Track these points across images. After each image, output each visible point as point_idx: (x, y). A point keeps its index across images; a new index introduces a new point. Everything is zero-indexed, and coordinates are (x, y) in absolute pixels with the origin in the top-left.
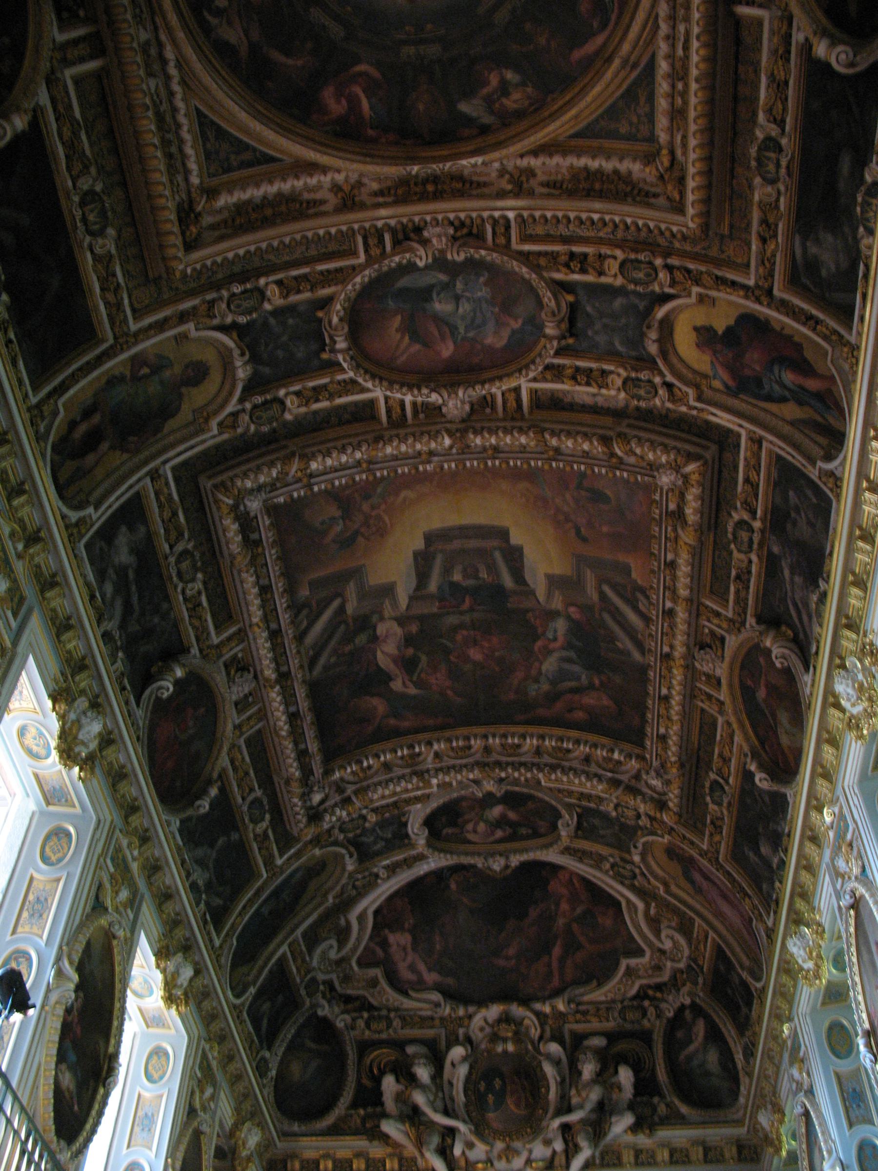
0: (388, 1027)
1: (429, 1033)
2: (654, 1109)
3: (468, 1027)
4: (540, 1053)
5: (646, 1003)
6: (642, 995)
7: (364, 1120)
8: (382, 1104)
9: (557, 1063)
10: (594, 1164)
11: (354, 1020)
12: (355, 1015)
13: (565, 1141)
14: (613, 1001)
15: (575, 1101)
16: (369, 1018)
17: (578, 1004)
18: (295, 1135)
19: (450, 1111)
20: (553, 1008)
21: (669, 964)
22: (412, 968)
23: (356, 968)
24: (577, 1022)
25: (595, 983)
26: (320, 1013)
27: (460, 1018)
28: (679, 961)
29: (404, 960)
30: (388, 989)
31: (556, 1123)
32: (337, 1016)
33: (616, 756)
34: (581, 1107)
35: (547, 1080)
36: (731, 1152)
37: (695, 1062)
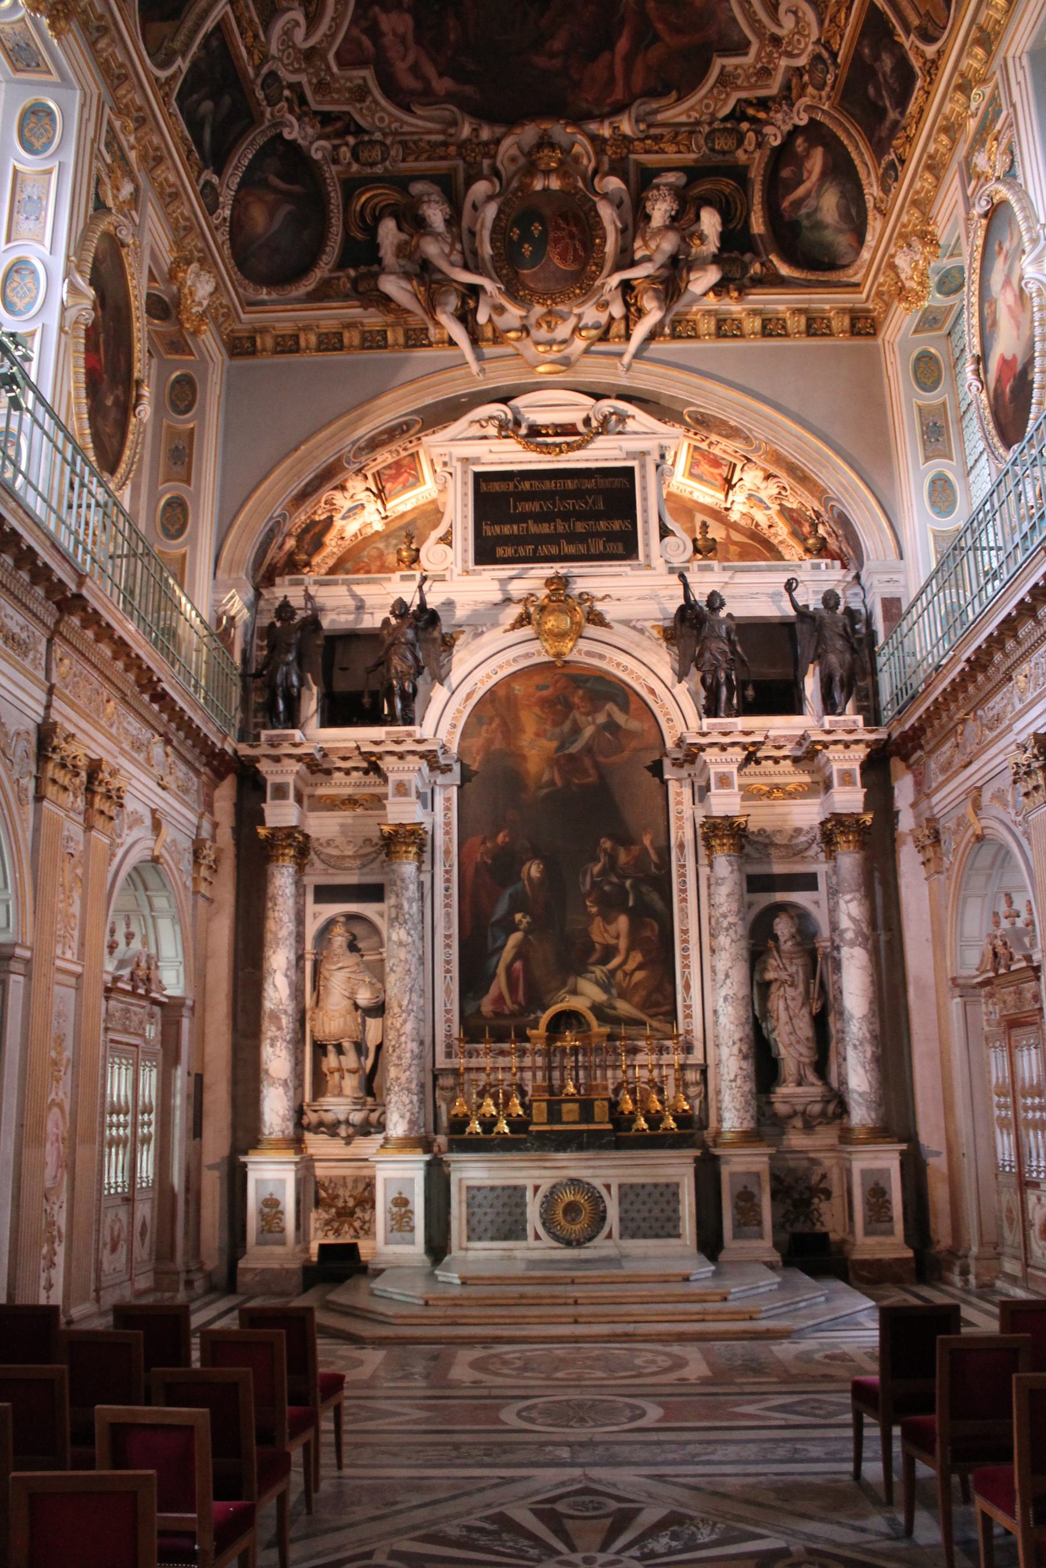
0: (384, 160)
2: (745, 268)
3: (494, 157)
4: (597, 194)
5: (745, 126)
6: (737, 115)
7: (355, 282)
8: (379, 261)
10: (662, 334)
11: (336, 148)
12: (336, 142)
13: (627, 305)
14: (698, 123)
15: (638, 255)
16: (356, 145)
17: (650, 126)
18: (263, 303)
19: (471, 265)
21: (784, 62)
22: (415, 70)
23: (335, 69)
24: (647, 152)
25: (674, 95)
26: (287, 136)
27: (486, 144)
28: (798, 55)
29: (403, 59)
30: (383, 102)
31: (615, 280)
32: (311, 143)
34: (648, 259)
35: (603, 228)
37: (803, 211)
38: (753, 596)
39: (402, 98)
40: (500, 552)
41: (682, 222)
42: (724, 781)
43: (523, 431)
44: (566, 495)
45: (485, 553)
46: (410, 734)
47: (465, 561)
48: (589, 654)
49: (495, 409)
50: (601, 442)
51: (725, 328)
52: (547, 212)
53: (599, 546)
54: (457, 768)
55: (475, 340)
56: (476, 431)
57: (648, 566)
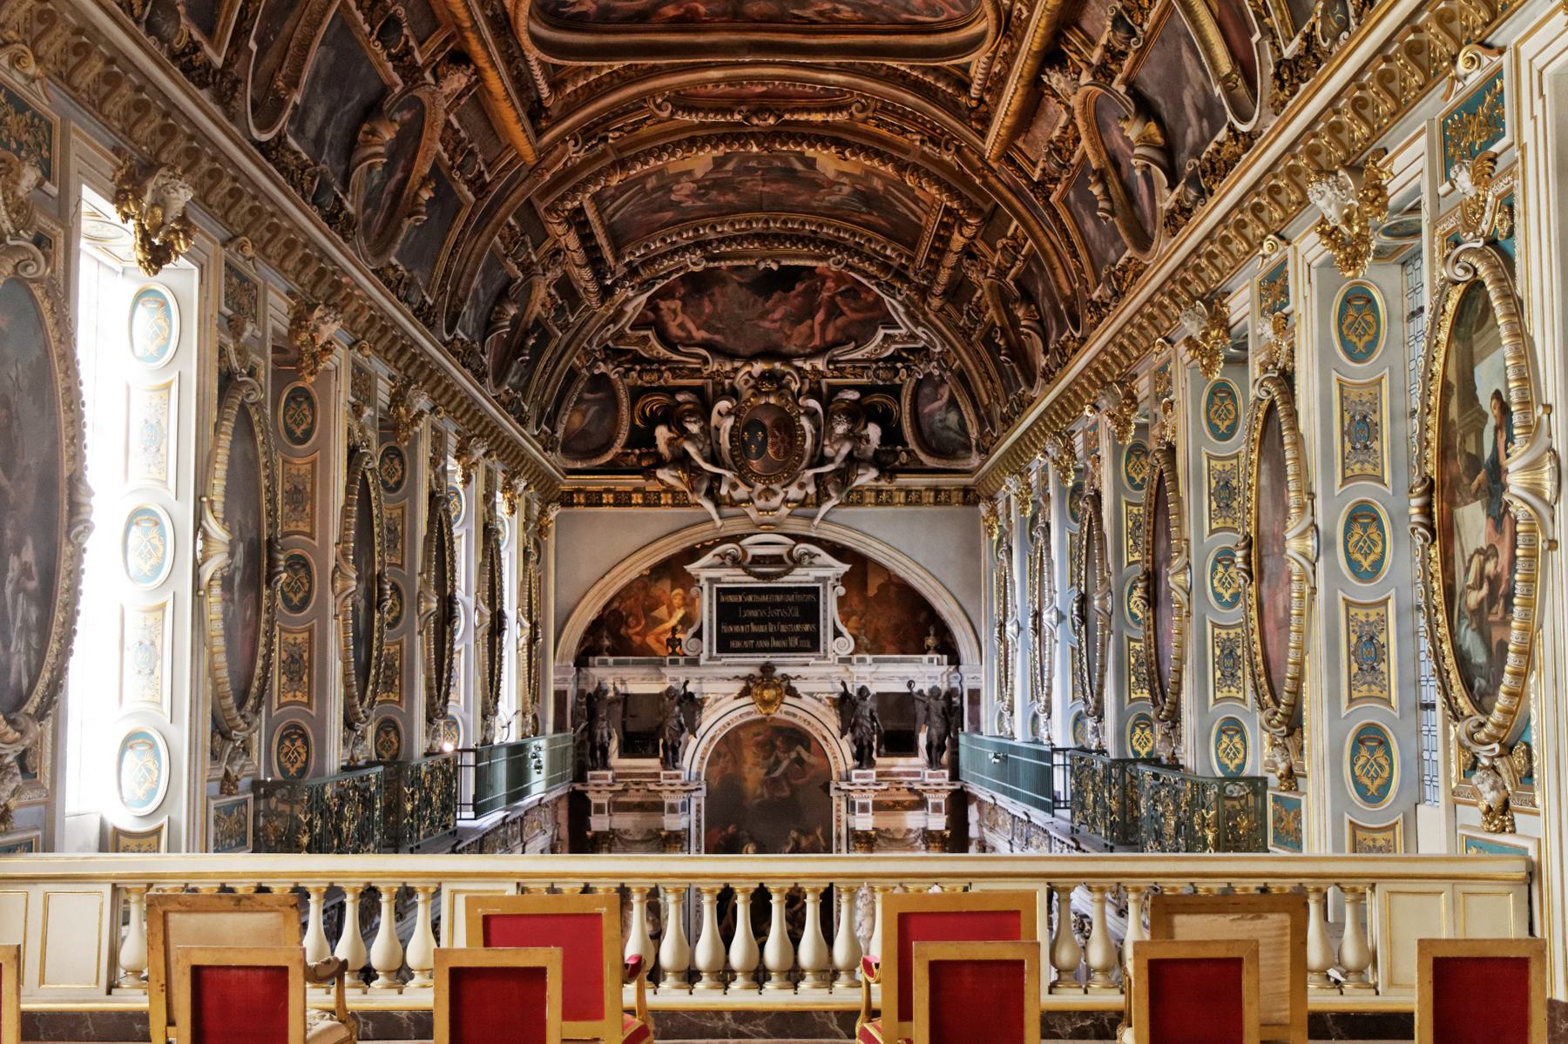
1: (699, 382)
5: (899, 365)
7: (640, 457)
9: (812, 414)
13: (817, 486)
20: (813, 367)
22: (681, 326)
26: (596, 372)
33: (888, 252)
36: (957, 496)
38: (891, 678)
39: (670, 344)
40: (732, 644)
41: (854, 437)
42: (864, 808)
43: (749, 559)
44: (775, 605)
45: (724, 645)
46: (678, 777)
47: (710, 651)
48: (787, 713)
49: (729, 547)
50: (798, 571)
51: (882, 498)
52: (767, 422)
53: (794, 642)
54: (704, 787)
55: (717, 505)
56: (718, 560)
57: (825, 658)
